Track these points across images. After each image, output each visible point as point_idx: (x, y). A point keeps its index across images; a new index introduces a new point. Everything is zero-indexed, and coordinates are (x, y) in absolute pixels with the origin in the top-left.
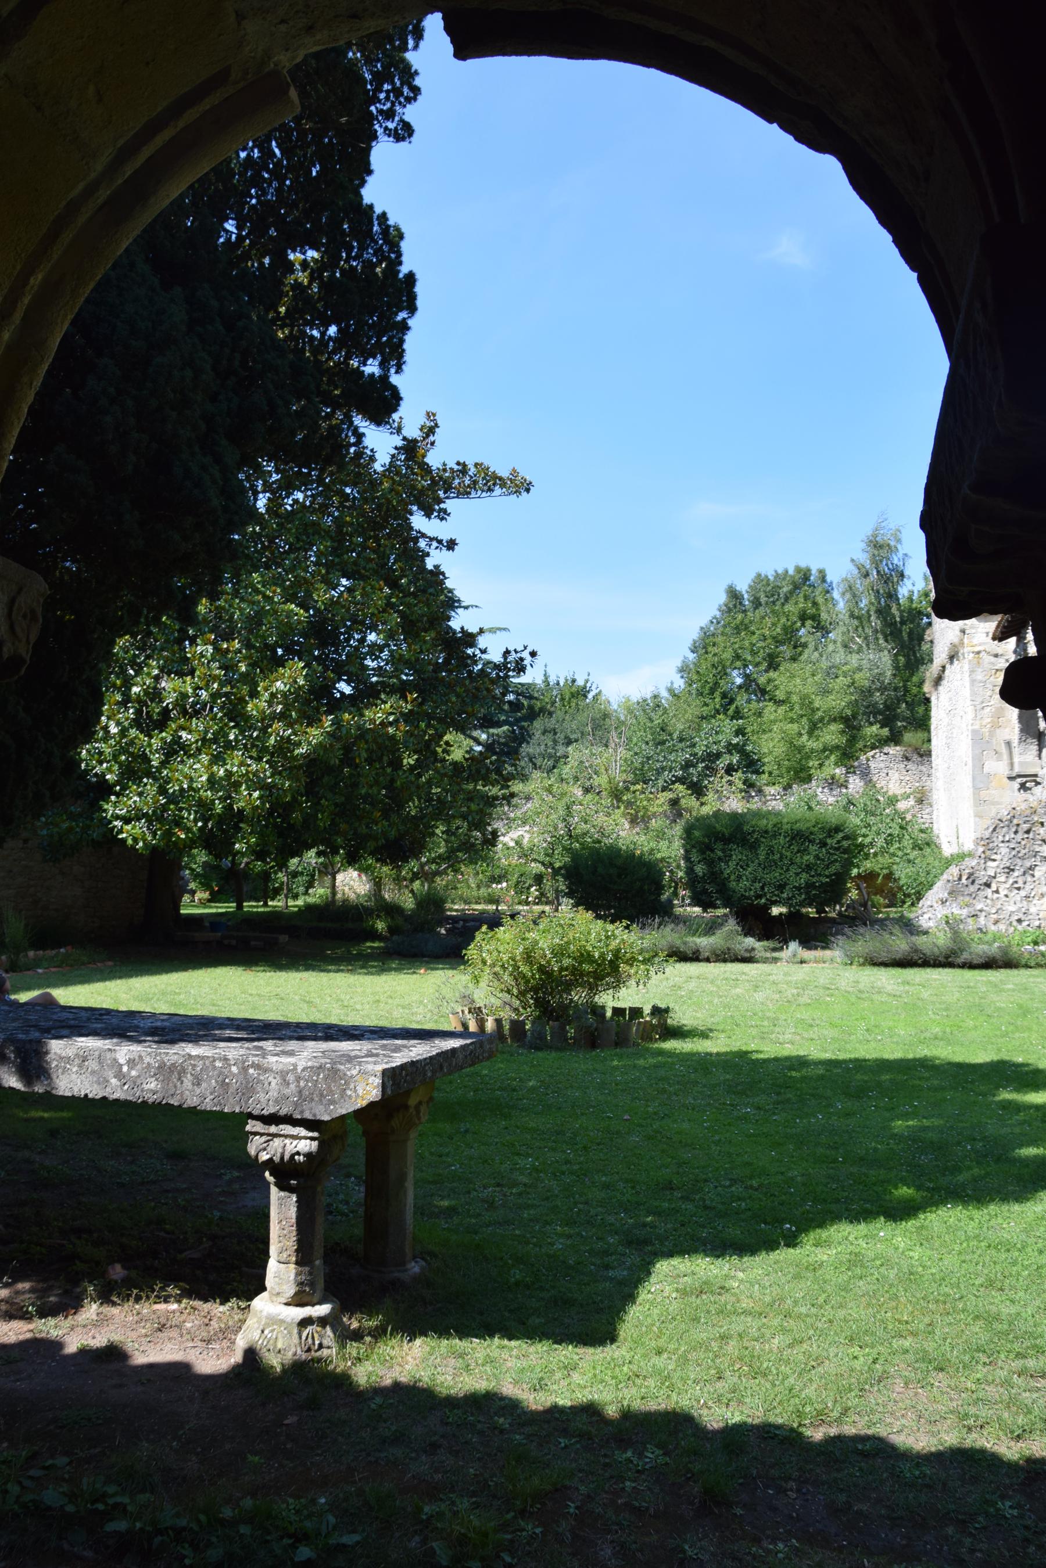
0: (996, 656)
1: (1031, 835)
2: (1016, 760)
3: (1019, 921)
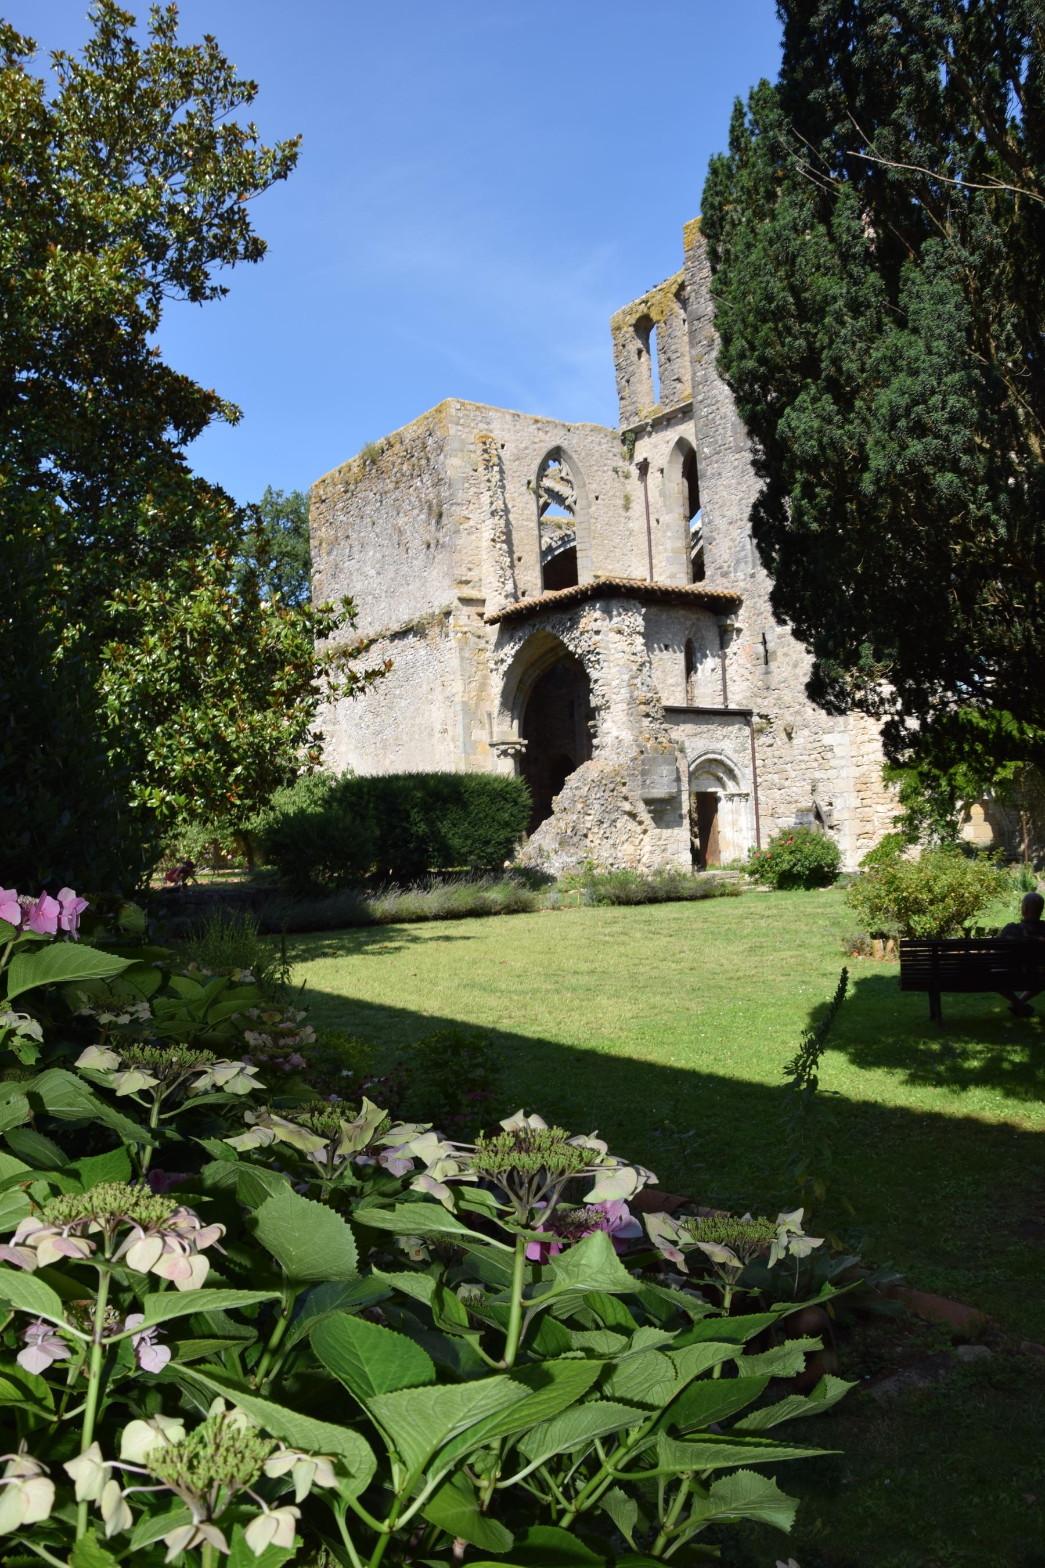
0: (479, 637)
2: (495, 729)
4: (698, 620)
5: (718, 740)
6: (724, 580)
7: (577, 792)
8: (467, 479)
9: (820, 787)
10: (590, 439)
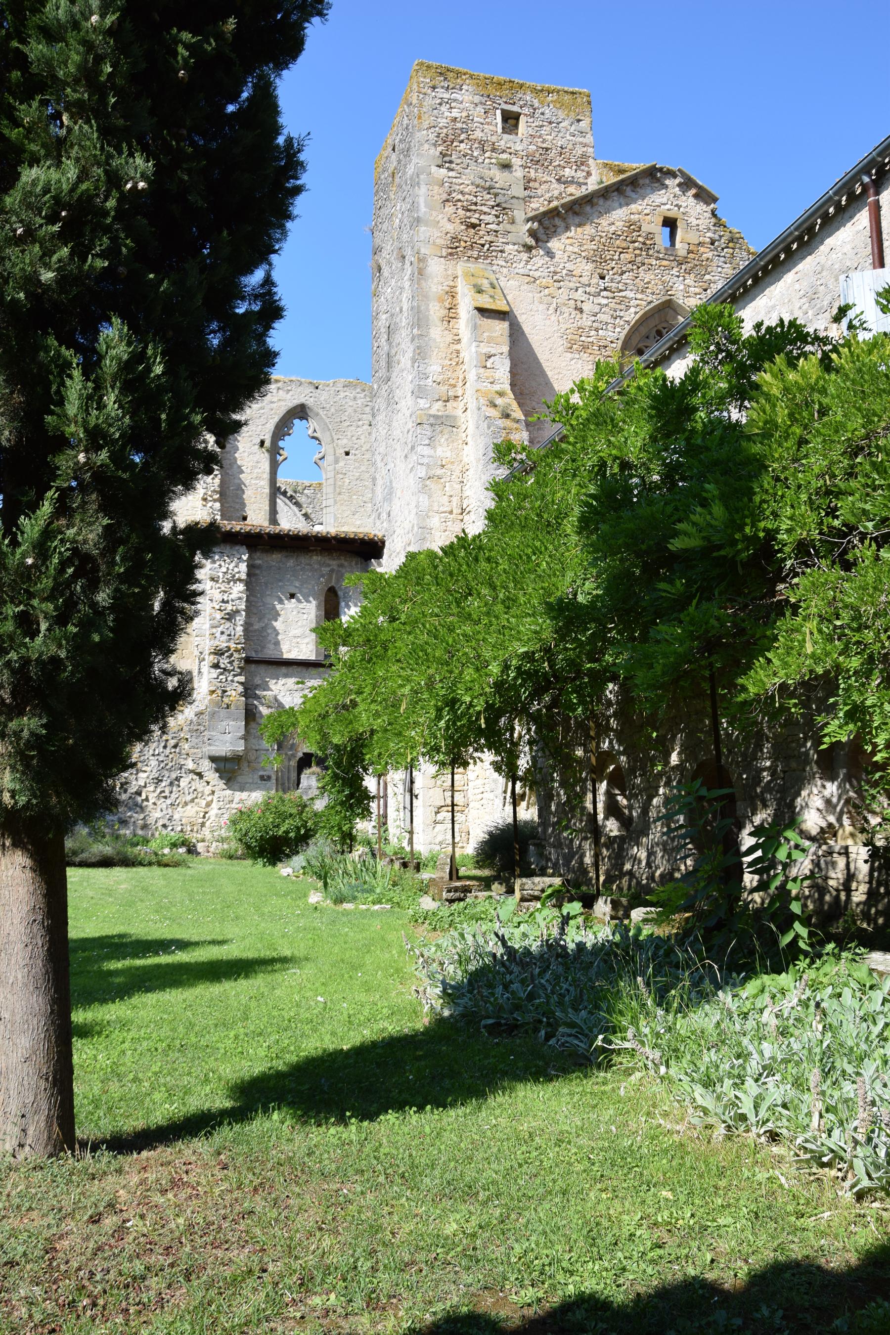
1: (177, 750)
3: (164, 826)
4: (341, 566)
10: (342, 394)
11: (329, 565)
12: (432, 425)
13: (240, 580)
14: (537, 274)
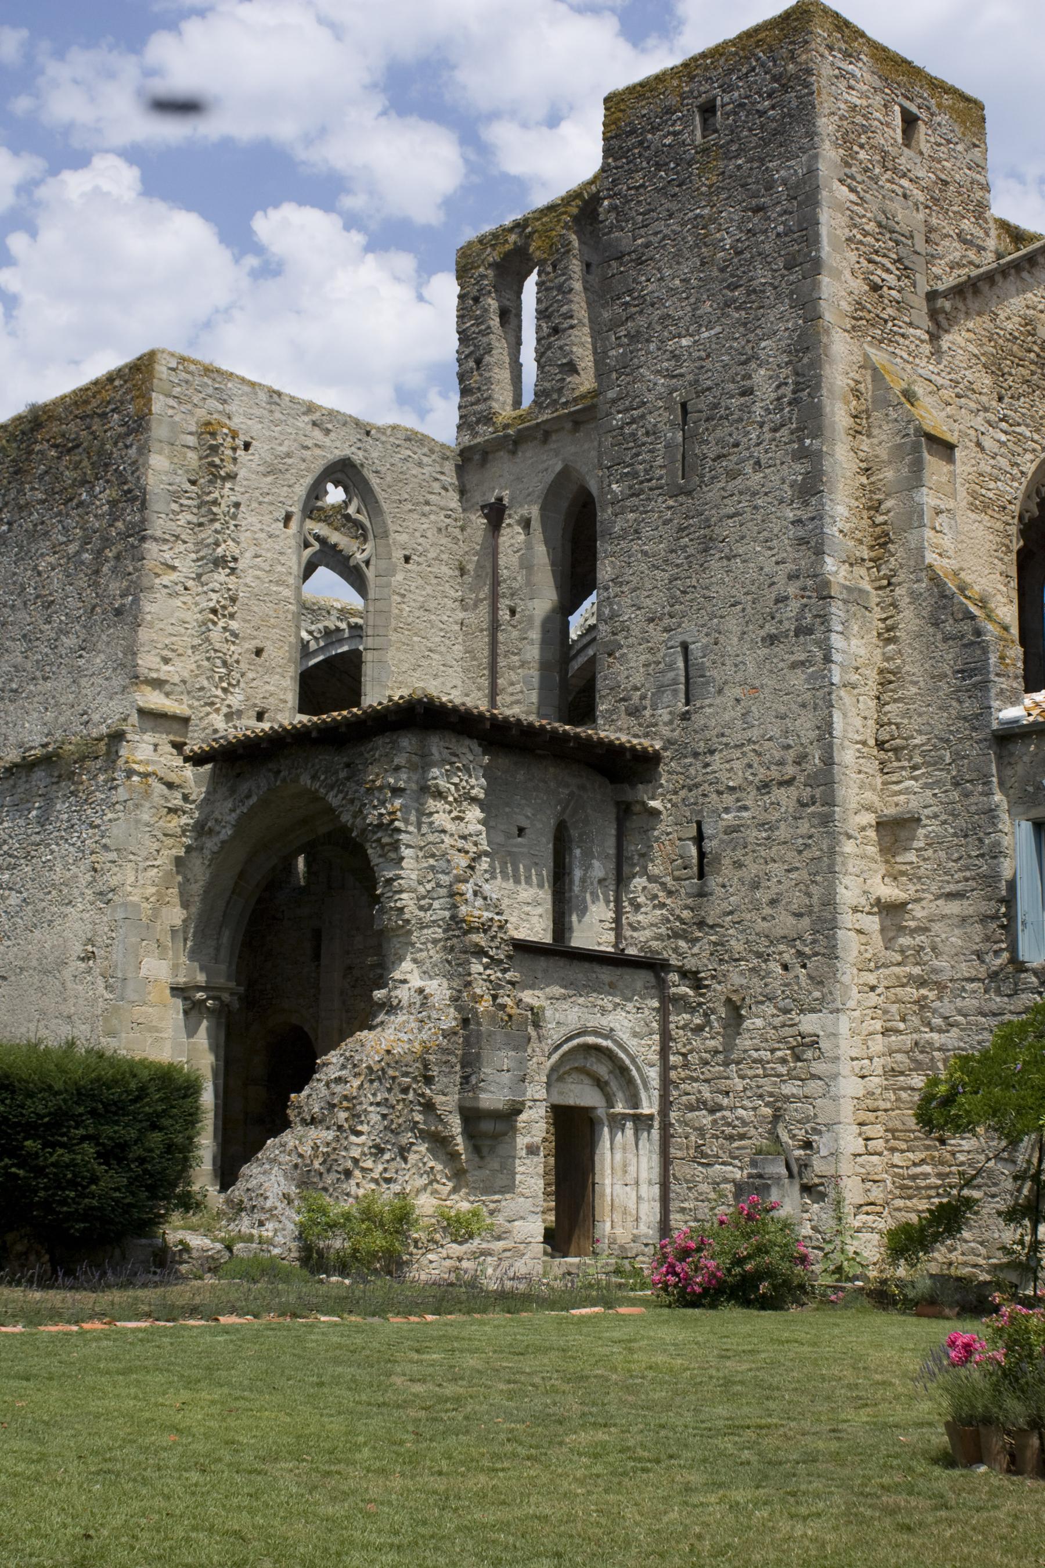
0: (170, 785)
5: (604, 1011)
6: (632, 721)
7: (338, 1089)
8: (175, 496)
9: (793, 1110)
11: (567, 786)
12: (845, 602)
13: (474, 800)
14: (940, 381)
